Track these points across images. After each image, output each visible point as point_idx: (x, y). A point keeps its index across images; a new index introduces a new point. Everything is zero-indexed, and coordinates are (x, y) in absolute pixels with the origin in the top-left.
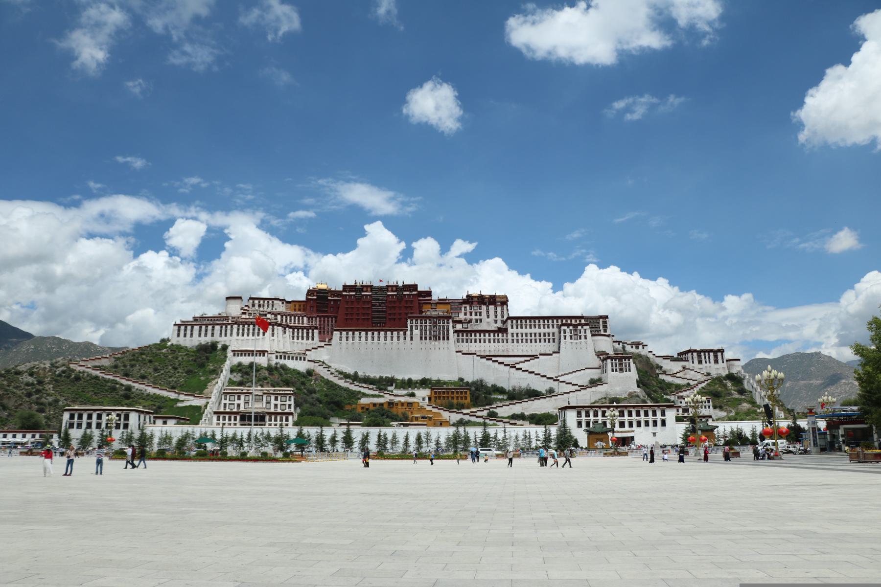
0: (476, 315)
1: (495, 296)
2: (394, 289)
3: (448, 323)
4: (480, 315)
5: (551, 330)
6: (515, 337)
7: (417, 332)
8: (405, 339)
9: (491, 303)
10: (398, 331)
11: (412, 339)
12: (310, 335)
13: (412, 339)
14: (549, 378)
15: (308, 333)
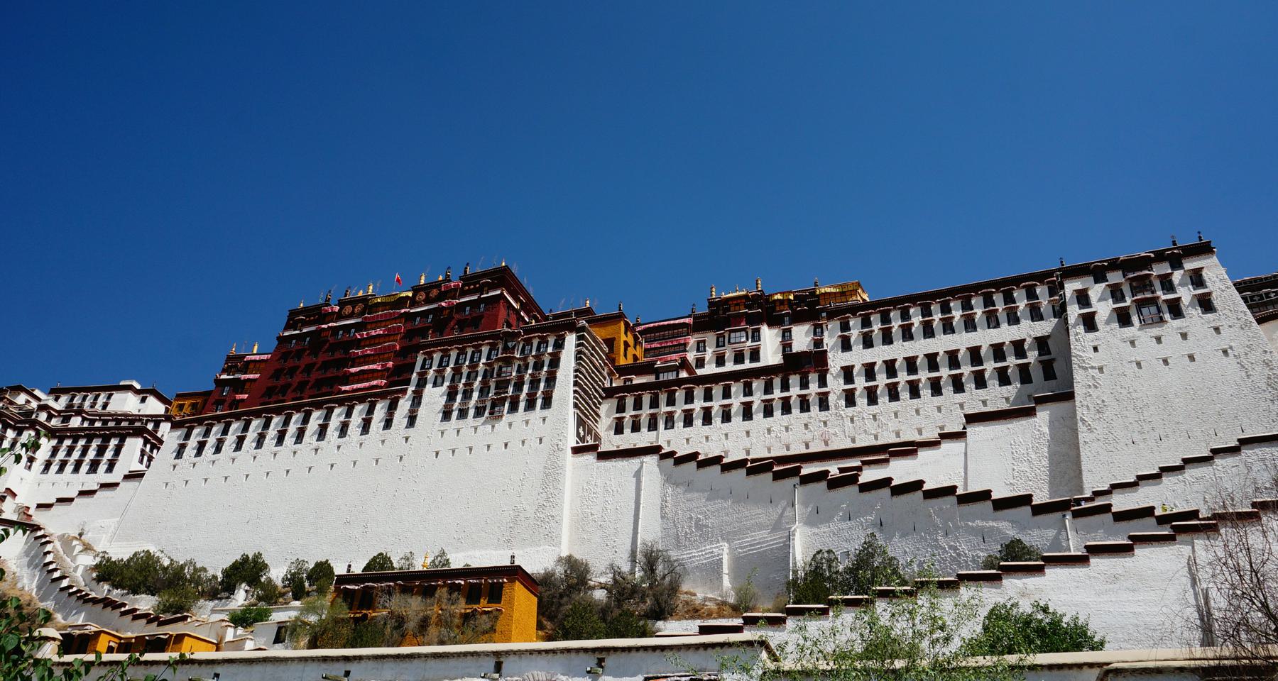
0: (739, 358)
1: (812, 293)
2: (435, 292)
3: (559, 345)
4: (755, 355)
5: (1028, 330)
6: (860, 383)
7: (434, 397)
8: (388, 424)
9: (798, 319)
10: (370, 399)
11: (412, 420)
12: (109, 454)
13: (412, 420)
14: (1003, 504)
15: (101, 451)
